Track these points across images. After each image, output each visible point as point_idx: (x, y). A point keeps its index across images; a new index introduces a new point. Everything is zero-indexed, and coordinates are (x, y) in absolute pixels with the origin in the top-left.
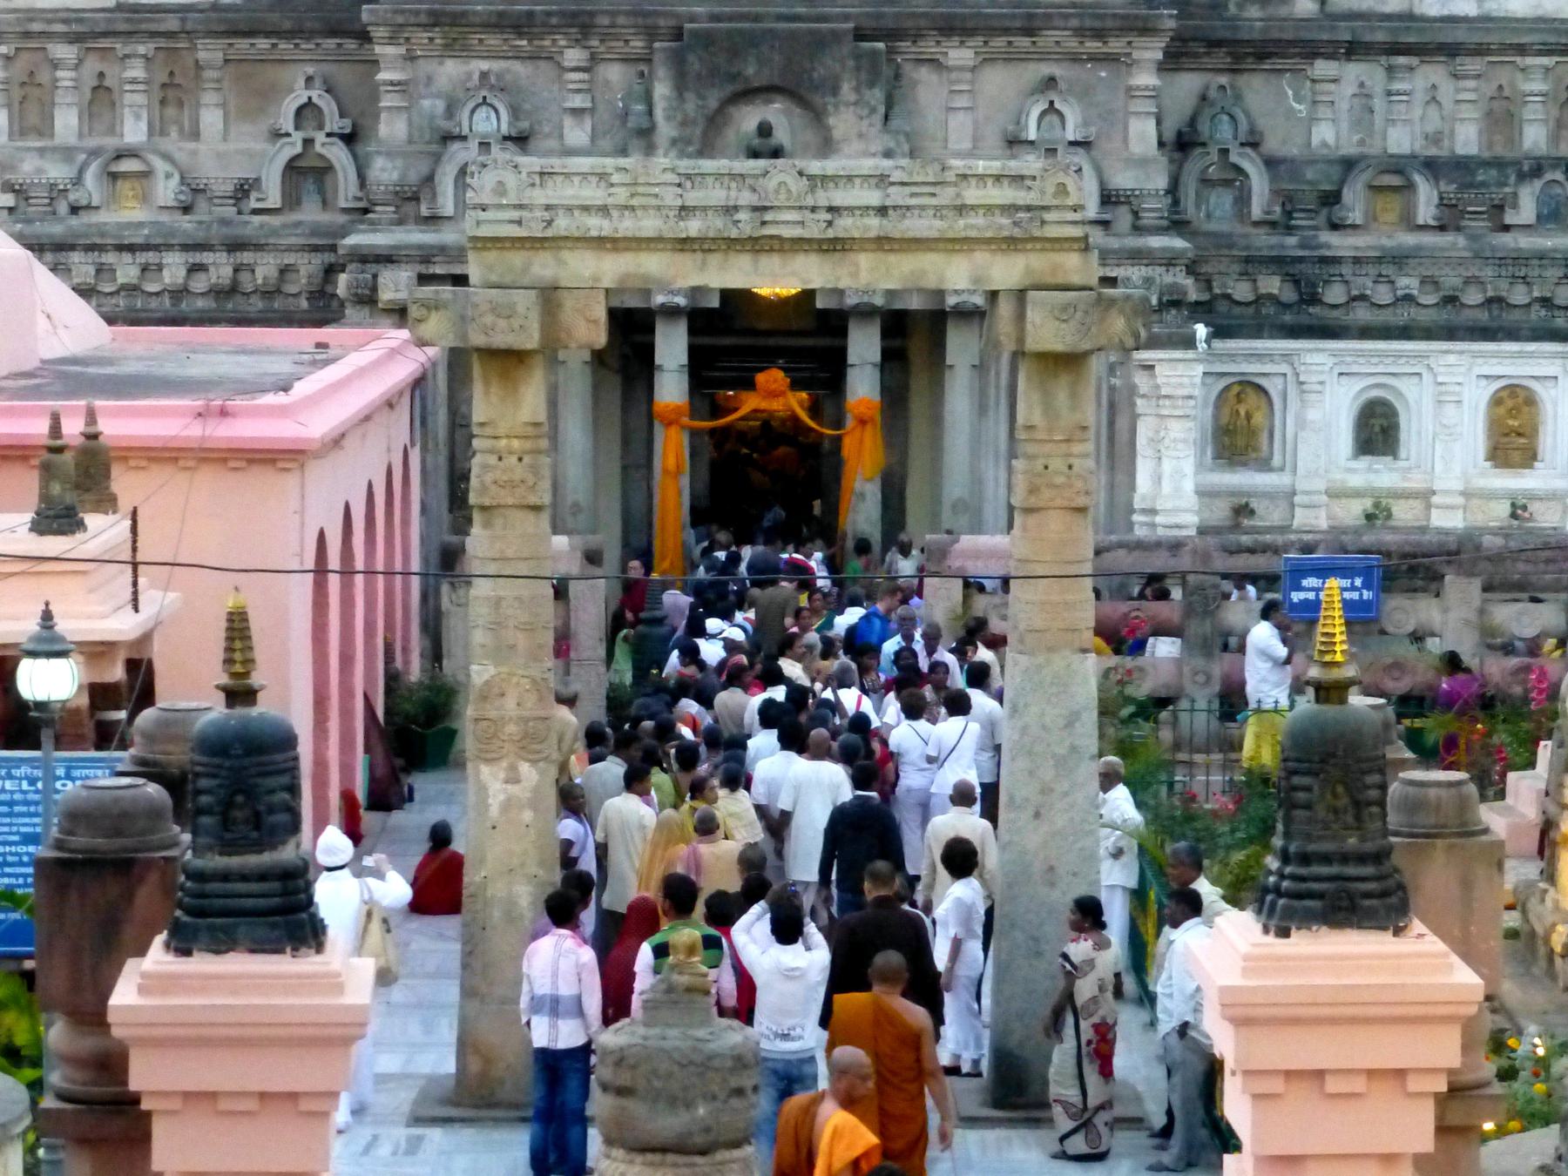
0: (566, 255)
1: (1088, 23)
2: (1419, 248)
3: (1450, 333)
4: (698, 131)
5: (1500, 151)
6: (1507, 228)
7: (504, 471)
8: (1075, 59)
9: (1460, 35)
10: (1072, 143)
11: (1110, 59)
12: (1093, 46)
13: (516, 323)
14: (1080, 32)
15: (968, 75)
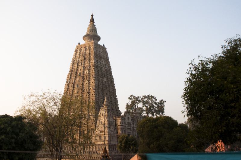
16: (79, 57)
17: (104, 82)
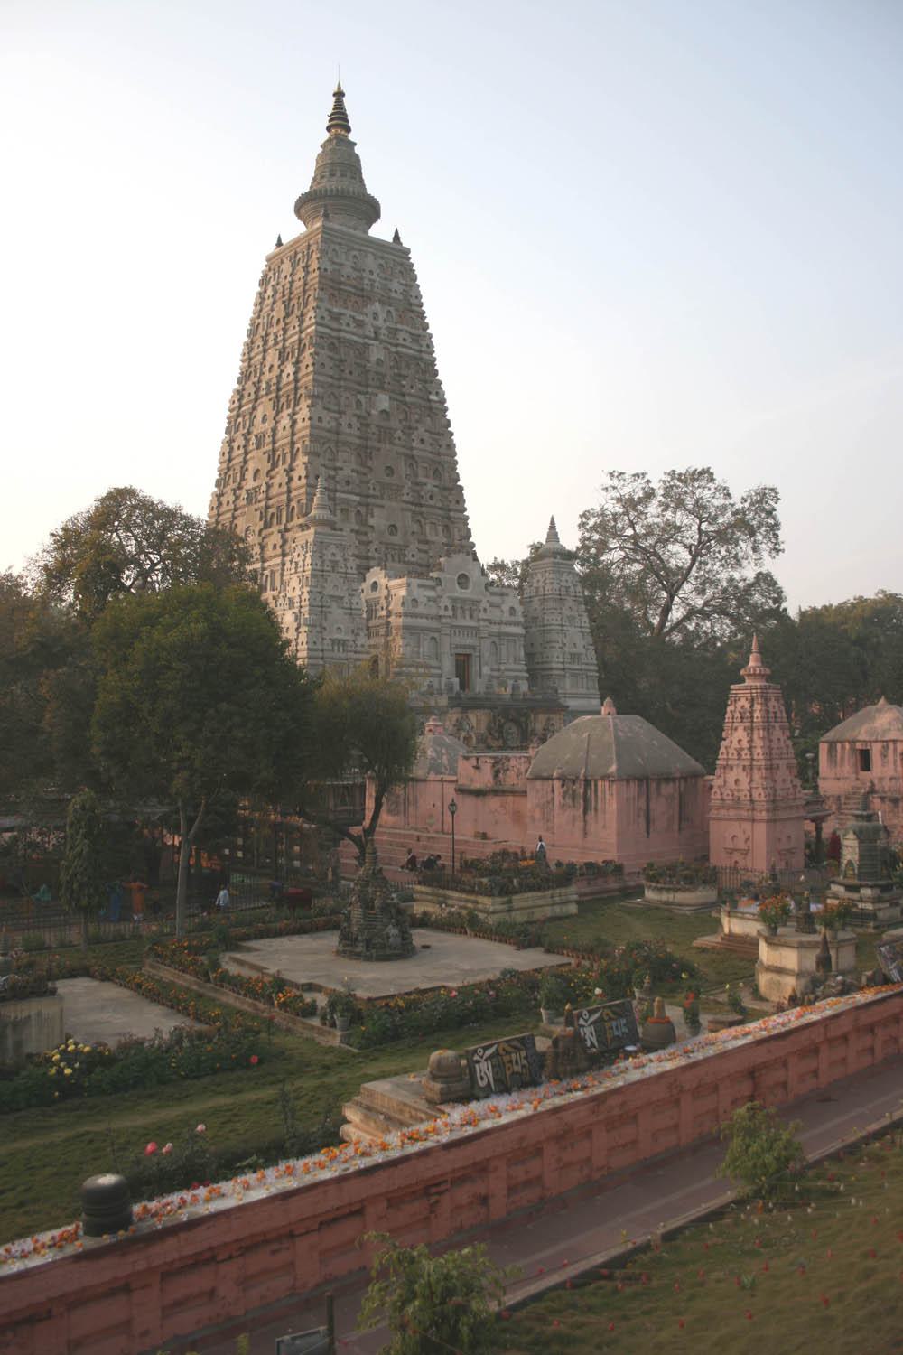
16: (272, 310)
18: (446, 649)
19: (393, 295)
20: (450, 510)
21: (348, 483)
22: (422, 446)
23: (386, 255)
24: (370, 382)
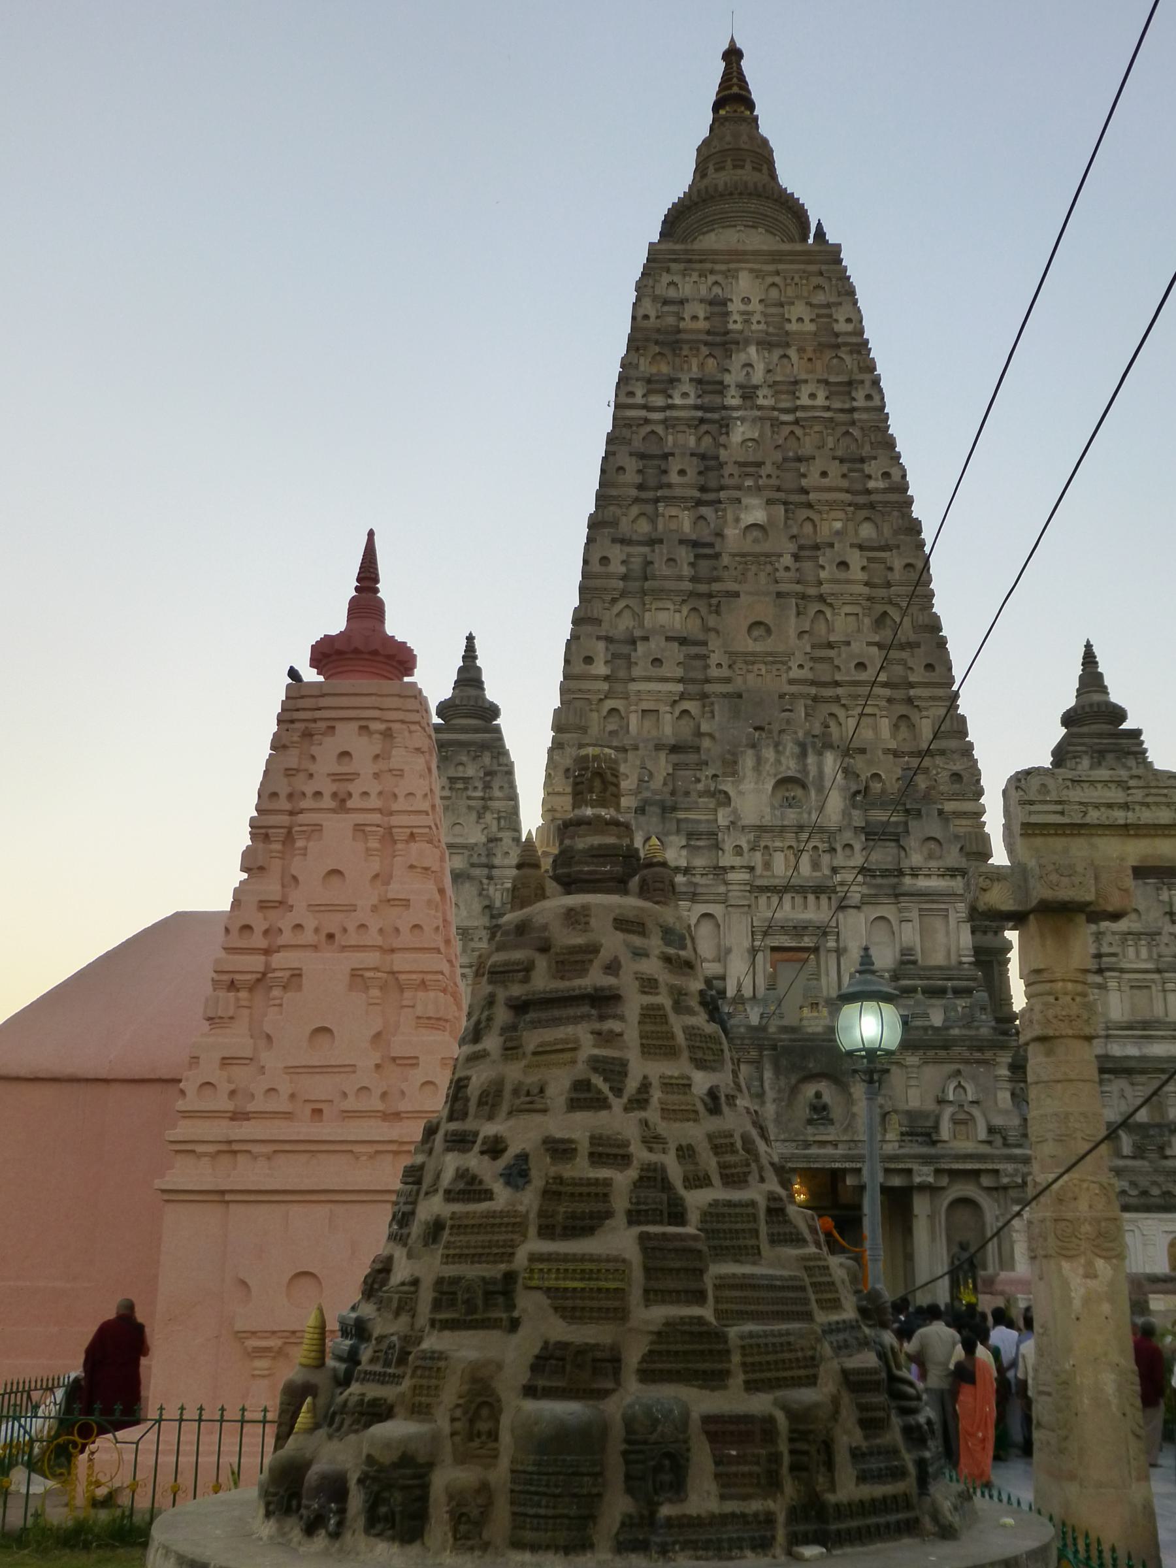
0: (1098, 841)
1: (975, 1043)
2: (1126, 1167)
3: (1148, 1209)
4: (787, 1095)
5: (1158, 1120)
6: (1166, 1157)
7: (1063, 1008)
8: (967, 1062)
9: (1133, 1064)
10: (972, 1102)
11: (985, 1062)
12: (977, 1055)
13: (1076, 880)
14: (970, 1048)
15: (915, 1070)
17: (731, 532)
18: (738, 936)
19: (793, 327)
20: (911, 685)
21: (657, 662)
22: (842, 575)
23: (781, 267)
24: (727, 481)
